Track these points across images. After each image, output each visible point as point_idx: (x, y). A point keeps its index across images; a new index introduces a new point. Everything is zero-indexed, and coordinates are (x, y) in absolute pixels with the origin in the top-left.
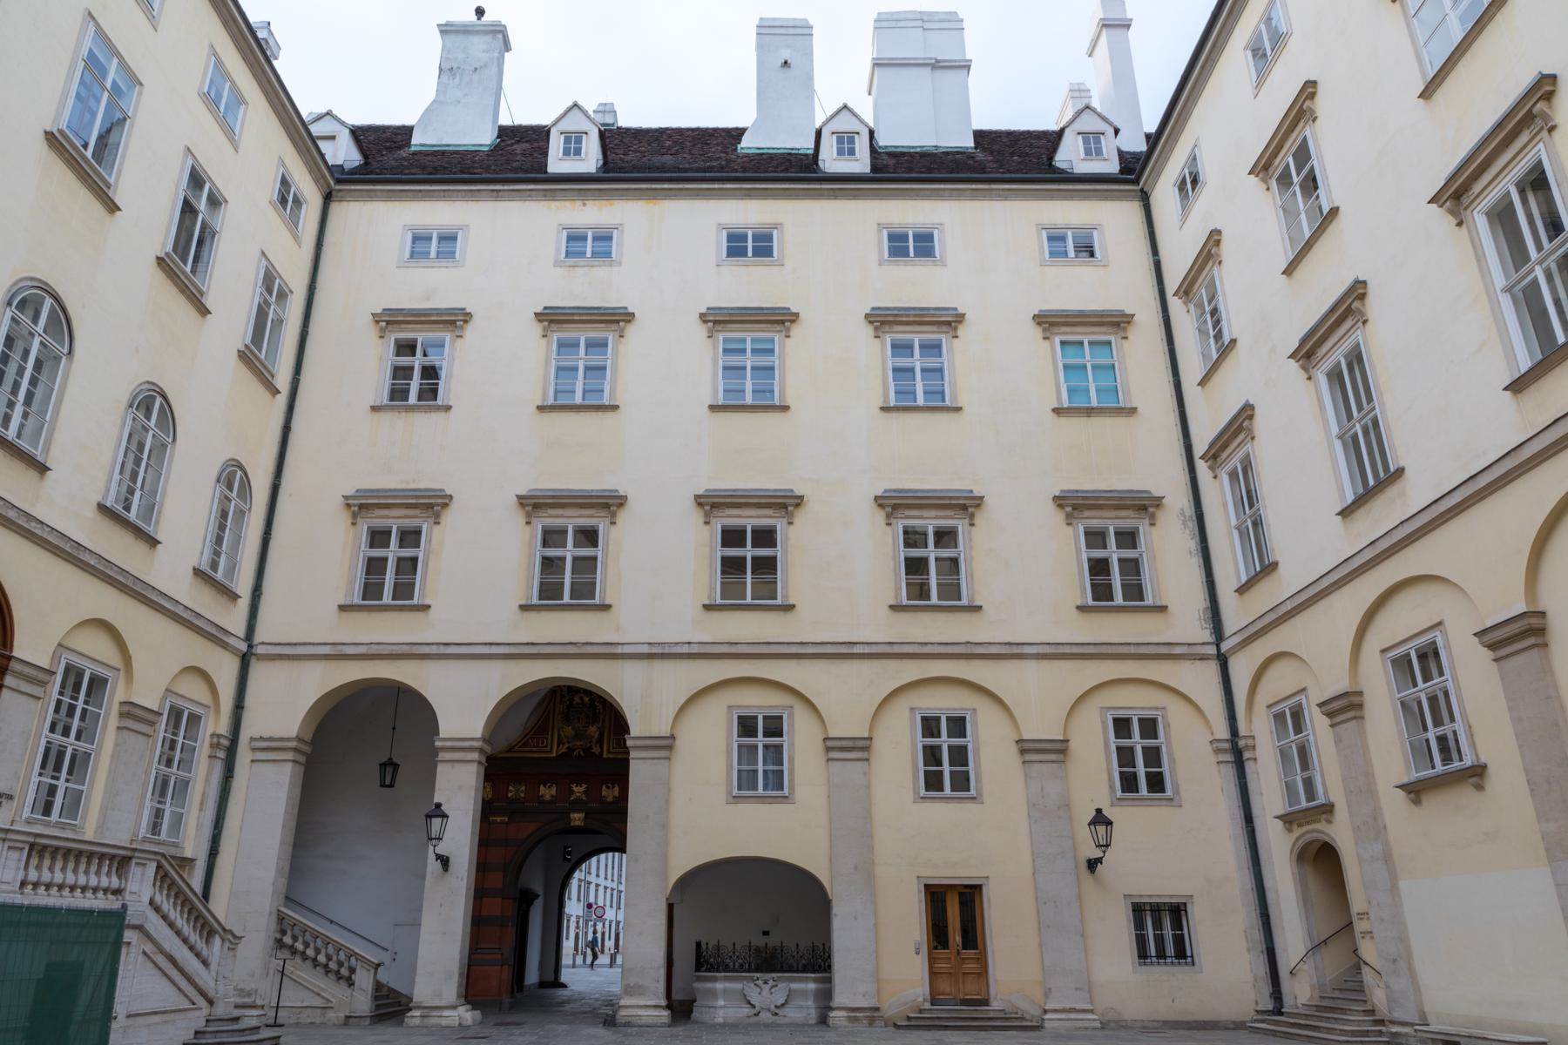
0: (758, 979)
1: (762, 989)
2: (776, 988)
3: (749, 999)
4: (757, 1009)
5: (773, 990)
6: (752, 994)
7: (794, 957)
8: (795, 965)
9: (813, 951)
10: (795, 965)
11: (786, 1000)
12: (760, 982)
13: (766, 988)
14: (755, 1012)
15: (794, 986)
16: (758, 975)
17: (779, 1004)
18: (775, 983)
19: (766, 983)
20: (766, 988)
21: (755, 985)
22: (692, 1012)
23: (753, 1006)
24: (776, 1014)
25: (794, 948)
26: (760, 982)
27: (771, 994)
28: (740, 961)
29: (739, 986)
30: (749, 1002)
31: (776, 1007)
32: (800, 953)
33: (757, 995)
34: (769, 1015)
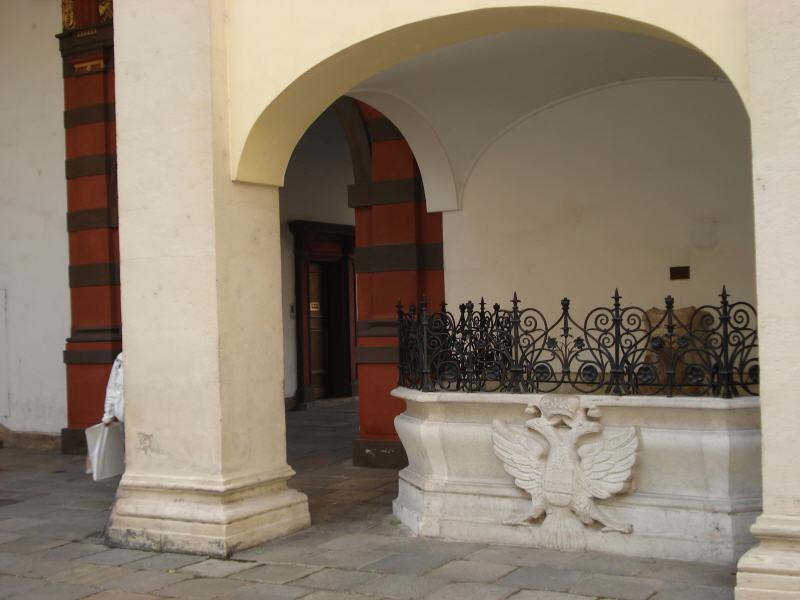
0: (538, 413)
2: (596, 444)
3: (513, 472)
4: (536, 505)
5: (584, 449)
6: (517, 457)
11: (630, 480)
12: (544, 424)
13: (562, 442)
15: (656, 437)
17: (604, 494)
18: (592, 426)
19: (561, 425)
20: (562, 442)
21: (530, 429)
23: (526, 496)
26: (544, 424)
28: (586, 355)
31: (596, 500)
33: (535, 462)
34: (572, 526)
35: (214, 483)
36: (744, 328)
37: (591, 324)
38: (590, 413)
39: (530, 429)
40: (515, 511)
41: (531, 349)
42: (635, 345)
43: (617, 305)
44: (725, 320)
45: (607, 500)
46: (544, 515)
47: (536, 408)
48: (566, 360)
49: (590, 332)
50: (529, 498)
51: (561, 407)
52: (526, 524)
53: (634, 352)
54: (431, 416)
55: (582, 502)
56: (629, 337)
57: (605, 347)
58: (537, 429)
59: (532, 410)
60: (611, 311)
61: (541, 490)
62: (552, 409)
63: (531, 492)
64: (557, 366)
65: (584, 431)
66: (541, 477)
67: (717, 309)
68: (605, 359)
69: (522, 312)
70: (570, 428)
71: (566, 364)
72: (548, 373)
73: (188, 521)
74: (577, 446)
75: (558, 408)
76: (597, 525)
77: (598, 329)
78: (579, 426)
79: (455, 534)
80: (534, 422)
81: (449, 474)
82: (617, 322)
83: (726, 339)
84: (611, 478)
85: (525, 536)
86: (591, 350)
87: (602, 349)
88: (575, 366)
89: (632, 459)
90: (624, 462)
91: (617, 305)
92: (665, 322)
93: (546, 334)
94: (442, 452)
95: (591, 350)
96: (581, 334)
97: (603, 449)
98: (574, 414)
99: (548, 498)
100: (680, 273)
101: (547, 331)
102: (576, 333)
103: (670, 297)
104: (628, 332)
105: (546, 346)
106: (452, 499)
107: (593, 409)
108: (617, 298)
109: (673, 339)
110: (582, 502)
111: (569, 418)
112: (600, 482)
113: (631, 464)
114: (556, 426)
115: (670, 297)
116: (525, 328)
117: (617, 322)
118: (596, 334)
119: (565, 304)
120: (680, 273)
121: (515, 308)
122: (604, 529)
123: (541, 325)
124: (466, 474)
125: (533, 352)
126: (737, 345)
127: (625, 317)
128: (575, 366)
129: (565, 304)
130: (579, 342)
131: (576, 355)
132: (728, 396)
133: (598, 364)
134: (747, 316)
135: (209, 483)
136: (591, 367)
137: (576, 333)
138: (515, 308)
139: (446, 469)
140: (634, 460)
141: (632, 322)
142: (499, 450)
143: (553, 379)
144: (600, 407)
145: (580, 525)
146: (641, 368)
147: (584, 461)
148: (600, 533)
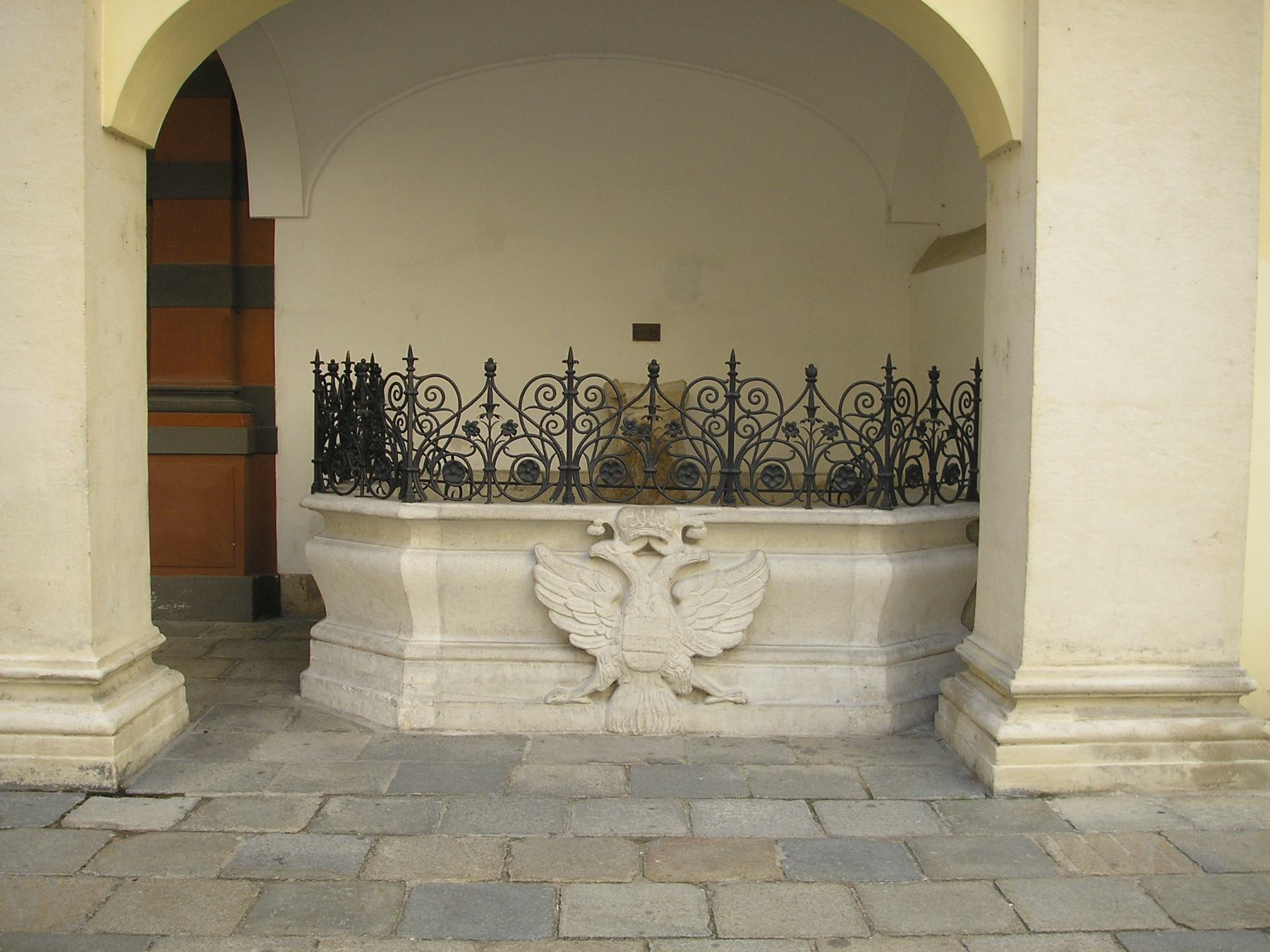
0: (609, 533)
1: (627, 582)
3: (566, 624)
4: (608, 670)
6: (573, 602)
7: (791, 429)
8: (796, 467)
9: (888, 403)
10: (796, 467)
11: (749, 630)
14: (600, 684)
16: (605, 513)
21: (597, 559)
22: (305, 661)
24: (700, 693)
25: (793, 387)
26: (619, 550)
27: (676, 601)
28: (521, 447)
29: (514, 566)
30: (563, 639)
31: (696, 658)
32: (823, 414)
33: (607, 608)
34: (661, 695)
35: (78, 664)
36: (438, 409)
37: (529, 400)
38: (689, 534)
39: (597, 559)
40: (563, 682)
41: (593, 436)
42: (759, 434)
43: (733, 375)
44: (411, 396)
45: (718, 657)
46: (615, 685)
47: (606, 525)
48: (810, 458)
49: (690, 413)
50: (593, 661)
51: (652, 524)
52: (585, 700)
53: (757, 444)
54: (414, 541)
55: (680, 661)
56: (750, 421)
57: (712, 436)
58: (611, 558)
59: (601, 530)
60: (722, 383)
61: (614, 649)
62: (636, 528)
63: (597, 653)
64: (477, 463)
65: (685, 560)
66: (617, 629)
67: (879, 386)
68: (712, 454)
69: (580, 380)
70: (661, 556)
71: (810, 465)
72: (781, 476)
73: (97, 734)
74: (673, 583)
75: (647, 526)
76: (700, 693)
77: (540, 407)
78: (674, 548)
79: (460, 723)
80: (602, 548)
81: (444, 631)
82: (732, 398)
83: (732, 427)
84: (725, 626)
85: (589, 718)
86: (849, 443)
87: (707, 437)
88: (503, 463)
89: (758, 597)
90: (744, 603)
91: (733, 375)
92: (805, 401)
93: (780, 419)
94: (435, 597)
95: (849, 443)
96: (516, 418)
97: (713, 587)
98: (670, 534)
99: (628, 660)
100: (646, 333)
101: (783, 414)
102: (506, 413)
103: (811, 366)
104: (749, 414)
105: (620, 433)
106: (455, 670)
107: (701, 528)
108: (733, 364)
109: (817, 425)
110: (680, 661)
111: (661, 539)
112: (709, 633)
113: (756, 605)
114: (637, 553)
115: (811, 366)
116: (586, 404)
117: (732, 398)
118: (537, 415)
119: (490, 369)
120: (646, 333)
121: (570, 374)
122: (710, 699)
123: (774, 406)
124: (472, 631)
125: (596, 441)
126: (589, 433)
127: (744, 393)
128: (503, 463)
129: (811, 375)
130: (830, 430)
131: (825, 451)
132: (890, 505)
133: (701, 460)
134: (766, 395)
135: (68, 664)
136: (692, 465)
137: (506, 413)
138: (570, 374)
139: (437, 622)
140: (759, 602)
141: (756, 400)
142: (547, 594)
143: (788, 487)
144: (707, 523)
145: (672, 695)
146: (842, 468)
147: (684, 604)
148: (701, 707)
